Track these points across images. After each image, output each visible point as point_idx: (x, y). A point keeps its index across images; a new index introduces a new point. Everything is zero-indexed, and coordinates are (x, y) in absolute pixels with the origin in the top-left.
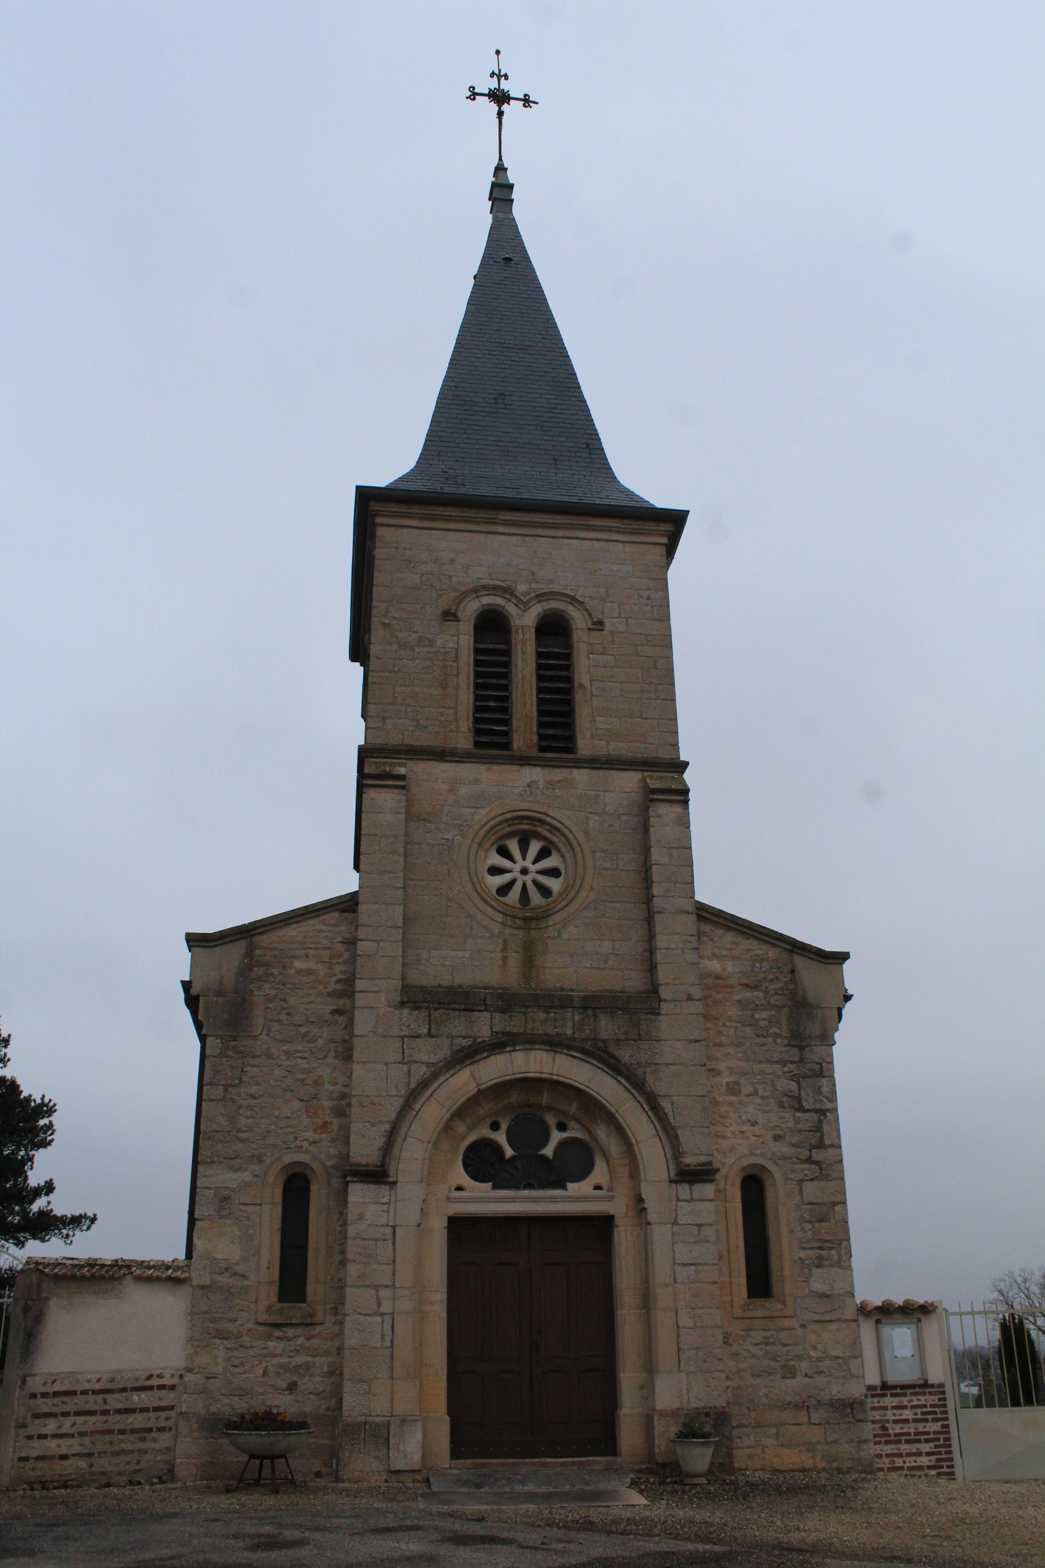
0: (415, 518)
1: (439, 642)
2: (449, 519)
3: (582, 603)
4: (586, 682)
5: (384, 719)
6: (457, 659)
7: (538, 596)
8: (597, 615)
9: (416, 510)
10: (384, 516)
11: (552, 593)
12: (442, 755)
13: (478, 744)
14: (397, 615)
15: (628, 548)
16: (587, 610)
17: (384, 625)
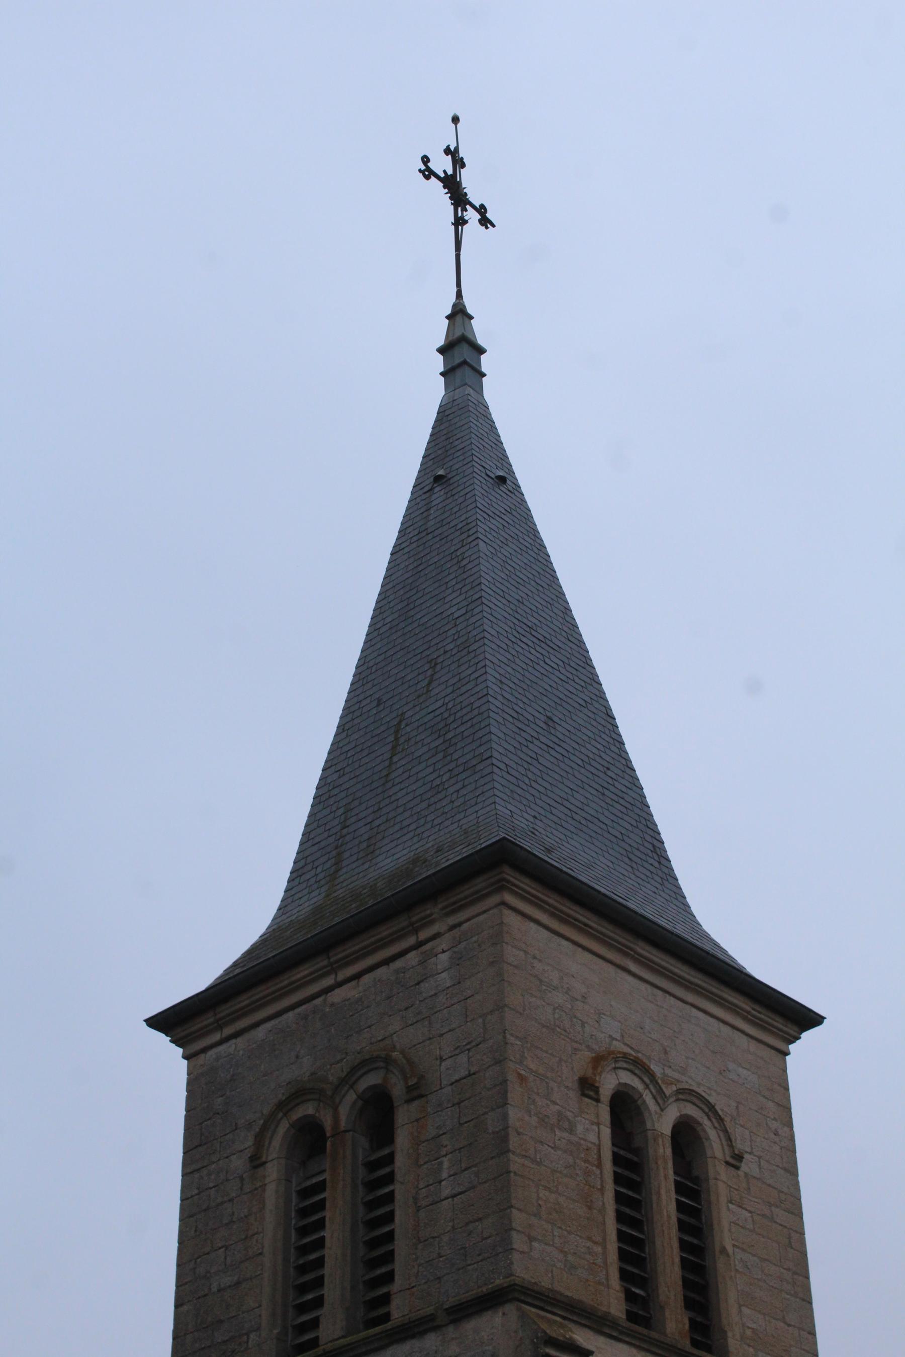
0: (545, 911)
1: (580, 1129)
2: (584, 929)
3: (720, 1119)
4: (730, 1249)
5: (531, 1239)
6: (599, 1165)
7: (680, 1091)
8: (739, 1145)
9: (553, 900)
10: (516, 894)
11: (691, 1092)
12: (599, 1322)
13: (631, 1316)
14: (532, 1066)
15: (753, 1046)
16: (726, 1131)
17: (522, 1079)
